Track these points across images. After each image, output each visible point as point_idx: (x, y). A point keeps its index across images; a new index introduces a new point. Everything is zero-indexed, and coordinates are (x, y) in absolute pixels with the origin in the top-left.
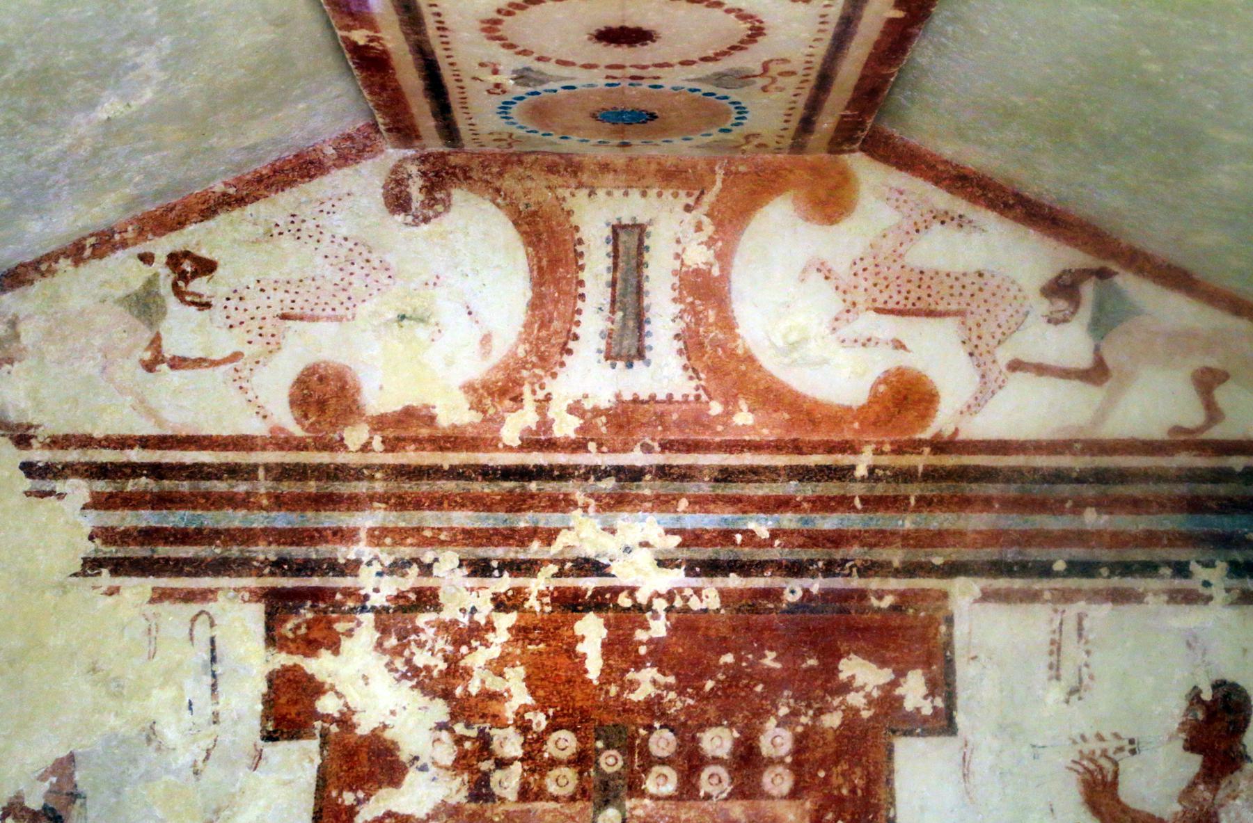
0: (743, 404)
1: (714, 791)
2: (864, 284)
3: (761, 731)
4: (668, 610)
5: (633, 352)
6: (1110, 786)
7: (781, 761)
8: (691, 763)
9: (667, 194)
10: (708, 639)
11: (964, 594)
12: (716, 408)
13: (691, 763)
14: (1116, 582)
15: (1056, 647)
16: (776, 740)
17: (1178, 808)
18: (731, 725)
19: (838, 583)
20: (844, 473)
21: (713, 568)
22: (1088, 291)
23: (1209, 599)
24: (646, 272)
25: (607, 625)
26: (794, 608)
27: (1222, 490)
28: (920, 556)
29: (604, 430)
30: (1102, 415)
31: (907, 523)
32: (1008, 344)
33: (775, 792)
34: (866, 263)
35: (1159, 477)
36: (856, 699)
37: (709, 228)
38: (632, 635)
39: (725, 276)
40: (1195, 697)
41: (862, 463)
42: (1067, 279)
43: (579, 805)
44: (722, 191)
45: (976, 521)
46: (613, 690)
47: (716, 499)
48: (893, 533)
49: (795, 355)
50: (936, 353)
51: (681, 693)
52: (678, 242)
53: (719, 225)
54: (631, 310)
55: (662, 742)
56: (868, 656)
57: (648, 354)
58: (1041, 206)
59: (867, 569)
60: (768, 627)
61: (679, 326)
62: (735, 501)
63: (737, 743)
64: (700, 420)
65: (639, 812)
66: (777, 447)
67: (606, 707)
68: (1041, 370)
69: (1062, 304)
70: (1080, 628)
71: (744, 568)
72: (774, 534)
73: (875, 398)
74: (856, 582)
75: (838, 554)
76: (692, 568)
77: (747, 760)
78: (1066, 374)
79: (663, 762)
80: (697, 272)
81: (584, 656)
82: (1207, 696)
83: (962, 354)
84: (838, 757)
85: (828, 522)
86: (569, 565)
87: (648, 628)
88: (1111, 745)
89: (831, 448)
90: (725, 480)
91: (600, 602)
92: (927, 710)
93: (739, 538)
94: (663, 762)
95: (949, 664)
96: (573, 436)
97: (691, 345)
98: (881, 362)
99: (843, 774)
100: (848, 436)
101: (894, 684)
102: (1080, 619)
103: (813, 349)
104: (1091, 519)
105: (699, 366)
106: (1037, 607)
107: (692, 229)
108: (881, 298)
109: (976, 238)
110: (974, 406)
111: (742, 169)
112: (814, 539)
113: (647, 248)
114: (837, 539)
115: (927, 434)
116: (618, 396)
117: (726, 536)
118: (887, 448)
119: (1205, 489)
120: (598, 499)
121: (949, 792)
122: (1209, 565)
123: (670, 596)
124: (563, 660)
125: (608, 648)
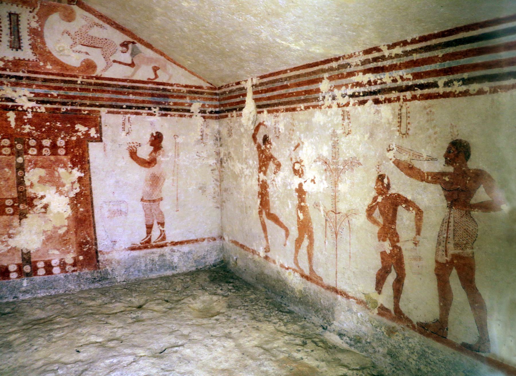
0: (49, 63)
1: (46, 154)
2: (78, 38)
3: (57, 140)
4: (32, 112)
5: (18, 47)
6: (135, 153)
7: (62, 147)
8: (40, 147)
9: (24, 7)
10: (43, 119)
11: (104, 111)
12: (42, 64)
13: (40, 147)
14: (136, 111)
15: (124, 124)
16: (61, 142)
17: (149, 157)
18: (50, 139)
19: (74, 108)
20: (75, 82)
21: (43, 102)
22: (130, 46)
23: (155, 115)
24: (20, 27)
25: (16, 114)
26: (64, 113)
27: (158, 92)
28: (94, 102)
29: (11, 66)
30: (133, 74)
31: (90, 95)
32: (112, 56)
33: (61, 154)
34: (78, 33)
35: (145, 89)
36: (79, 134)
37: (37, 18)
38: (22, 117)
39: (42, 31)
40: (152, 135)
41: (79, 80)
42: (126, 43)
43: (11, 157)
44: (40, 9)
45: (106, 96)
46: (19, 130)
47: (43, 86)
48: (87, 97)
49: (61, 53)
50: (95, 55)
51: (37, 131)
52: (28, 20)
53: (40, 18)
54: (16, 36)
55: (32, 142)
56: (82, 124)
57: (22, 48)
58: (119, 25)
59: (81, 105)
60: (58, 117)
61: (30, 42)
62: (48, 87)
63: (51, 143)
64: (37, 66)
65: (27, 158)
66: (58, 75)
67: (17, 134)
68: (120, 63)
69: (125, 49)
70: (129, 120)
71: (51, 103)
72: (58, 95)
73: (82, 65)
74: (79, 108)
75: (74, 101)
76: (37, 102)
77: (54, 147)
78: (126, 64)
79: (33, 147)
80: (34, 29)
81: (10, 122)
82: (155, 135)
83: (102, 57)
84: (76, 146)
85: (72, 93)
86: (4, 99)
87: (27, 116)
88: (135, 145)
89: (71, 76)
90: (45, 81)
91: (13, 109)
92: (96, 137)
93: (49, 96)
94: (33, 147)
95: (101, 126)
96: (2, 67)
97: (34, 47)
98: (84, 57)
99: (77, 150)
100: (76, 74)
101: (88, 131)
102: (129, 118)
103: (66, 52)
104: (131, 97)
105: (36, 53)
106: (119, 115)
107: (32, 17)
108: (83, 42)
109: (105, 31)
110: (105, 70)
111: (45, 4)
112: (68, 97)
113: (20, 21)
114: (74, 97)
115: (94, 75)
116: (14, 58)
117: (46, 95)
118: (85, 77)
119: (155, 92)
120: (11, 83)
121: (101, 155)
122: (155, 108)
123: (32, 108)
124: (4, 122)
125: (16, 120)
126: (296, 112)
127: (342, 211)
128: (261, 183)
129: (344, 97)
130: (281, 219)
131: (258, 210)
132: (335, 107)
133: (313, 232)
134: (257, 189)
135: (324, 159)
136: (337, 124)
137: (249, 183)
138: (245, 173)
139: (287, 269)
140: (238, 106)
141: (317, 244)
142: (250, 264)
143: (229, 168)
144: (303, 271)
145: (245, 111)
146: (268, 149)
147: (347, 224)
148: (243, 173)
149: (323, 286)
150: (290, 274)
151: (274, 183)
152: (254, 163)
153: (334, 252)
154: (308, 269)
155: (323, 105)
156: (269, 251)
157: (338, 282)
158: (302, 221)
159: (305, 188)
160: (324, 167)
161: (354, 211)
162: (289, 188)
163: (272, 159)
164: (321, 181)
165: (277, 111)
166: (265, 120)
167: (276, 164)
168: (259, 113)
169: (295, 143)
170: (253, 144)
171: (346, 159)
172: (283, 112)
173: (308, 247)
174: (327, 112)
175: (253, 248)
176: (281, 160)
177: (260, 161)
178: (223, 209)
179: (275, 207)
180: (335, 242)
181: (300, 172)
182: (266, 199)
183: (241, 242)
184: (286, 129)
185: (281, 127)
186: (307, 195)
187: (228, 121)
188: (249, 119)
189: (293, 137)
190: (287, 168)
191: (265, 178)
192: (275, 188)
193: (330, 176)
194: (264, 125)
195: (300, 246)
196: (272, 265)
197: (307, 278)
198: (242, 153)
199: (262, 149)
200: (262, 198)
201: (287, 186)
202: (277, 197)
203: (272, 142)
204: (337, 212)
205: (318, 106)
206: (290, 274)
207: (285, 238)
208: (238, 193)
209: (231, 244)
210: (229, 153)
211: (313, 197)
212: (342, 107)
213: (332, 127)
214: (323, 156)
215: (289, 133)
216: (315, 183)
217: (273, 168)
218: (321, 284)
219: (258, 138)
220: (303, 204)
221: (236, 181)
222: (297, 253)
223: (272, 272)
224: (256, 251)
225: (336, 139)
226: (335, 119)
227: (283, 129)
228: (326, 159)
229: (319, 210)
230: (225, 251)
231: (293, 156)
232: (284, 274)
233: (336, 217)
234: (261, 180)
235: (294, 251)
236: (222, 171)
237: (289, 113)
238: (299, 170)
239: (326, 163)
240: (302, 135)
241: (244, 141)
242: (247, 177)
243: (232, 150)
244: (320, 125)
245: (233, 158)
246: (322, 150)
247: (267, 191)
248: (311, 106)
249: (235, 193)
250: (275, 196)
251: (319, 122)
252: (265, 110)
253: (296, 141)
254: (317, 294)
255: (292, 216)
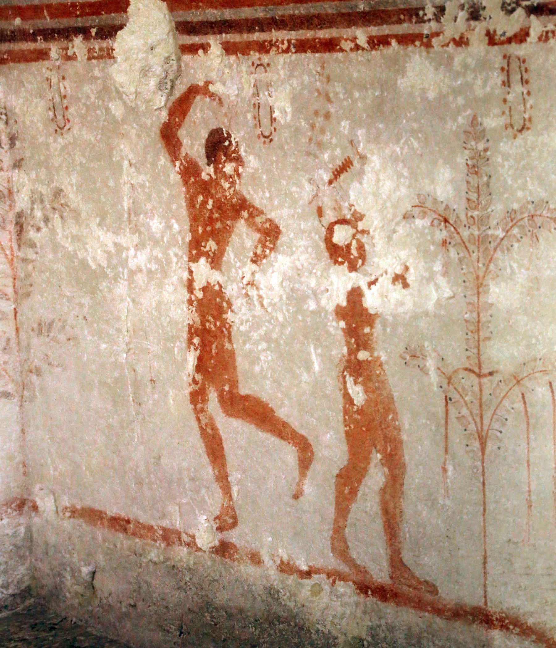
126: (340, 55)
127: (501, 368)
128: (200, 295)
129: (513, 11)
130: (282, 413)
131: (187, 391)
132: (478, 46)
133: (401, 442)
134: (183, 315)
135: (441, 209)
136: (487, 100)
137: (149, 300)
138: (132, 264)
139: (308, 574)
140: (93, 21)
141: (414, 478)
142: (155, 582)
143: (56, 247)
144: (366, 572)
145: (126, 42)
146: (226, 177)
147: (519, 406)
148: (124, 263)
149: (438, 611)
150: (317, 590)
151: (253, 293)
152: (169, 227)
153: (477, 497)
154: (385, 564)
155: (437, 34)
156: (235, 524)
157: (489, 589)
158: (361, 411)
159: (371, 301)
160: (441, 235)
161: (539, 363)
162: (312, 305)
163: (245, 214)
164: (431, 279)
165: (263, 47)
166: (213, 76)
167: (259, 230)
168: (192, 49)
169: (333, 159)
170: (164, 160)
171: (516, 206)
172: (287, 51)
173: (383, 491)
174: (451, 58)
175: (166, 523)
176: (280, 214)
177: (195, 219)
178: (32, 399)
179: (258, 370)
180: (479, 464)
181: (354, 252)
182: (221, 348)
183: (112, 511)
184: (297, 111)
185: (281, 104)
186: (378, 326)
187: (48, 74)
188: (145, 72)
189: (326, 138)
190: (302, 243)
191: (216, 277)
192: (258, 310)
193: (461, 261)
194: (212, 95)
195: (354, 492)
196: (248, 570)
197: (382, 593)
198: (116, 192)
199: (204, 176)
200: (205, 346)
201: (304, 299)
202: (267, 338)
203: (242, 153)
204: (485, 371)
205: (420, 36)
206: (317, 590)
207: (296, 473)
208: (100, 334)
209: (67, 524)
210: (58, 193)
211: (400, 330)
212: (502, 43)
213: (465, 107)
214: (435, 200)
215: (313, 126)
216: (406, 285)
217: (249, 243)
218: (432, 604)
219: (186, 141)
220: (363, 355)
221: (93, 291)
222: (345, 518)
223: (249, 593)
224: (178, 534)
225: (481, 146)
226: (479, 82)
227: (289, 110)
228: (447, 207)
229: (424, 370)
230: (39, 552)
231: (327, 202)
232: (293, 595)
233: (480, 385)
234: (198, 285)
235: (331, 512)
236: (25, 260)
237: (311, 60)
238: (348, 246)
239: (446, 221)
240: (361, 133)
241: (125, 149)
242: (140, 279)
243: (69, 183)
244: (424, 99)
245: (76, 214)
246: (433, 181)
247: (224, 322)
248: (396, 36)
249: (87, 337)
250: (255, 335)
251: (424, 91)
252: (215, 43)
253: (338, 152)
254: (419, 639)
255: (326, 396)
